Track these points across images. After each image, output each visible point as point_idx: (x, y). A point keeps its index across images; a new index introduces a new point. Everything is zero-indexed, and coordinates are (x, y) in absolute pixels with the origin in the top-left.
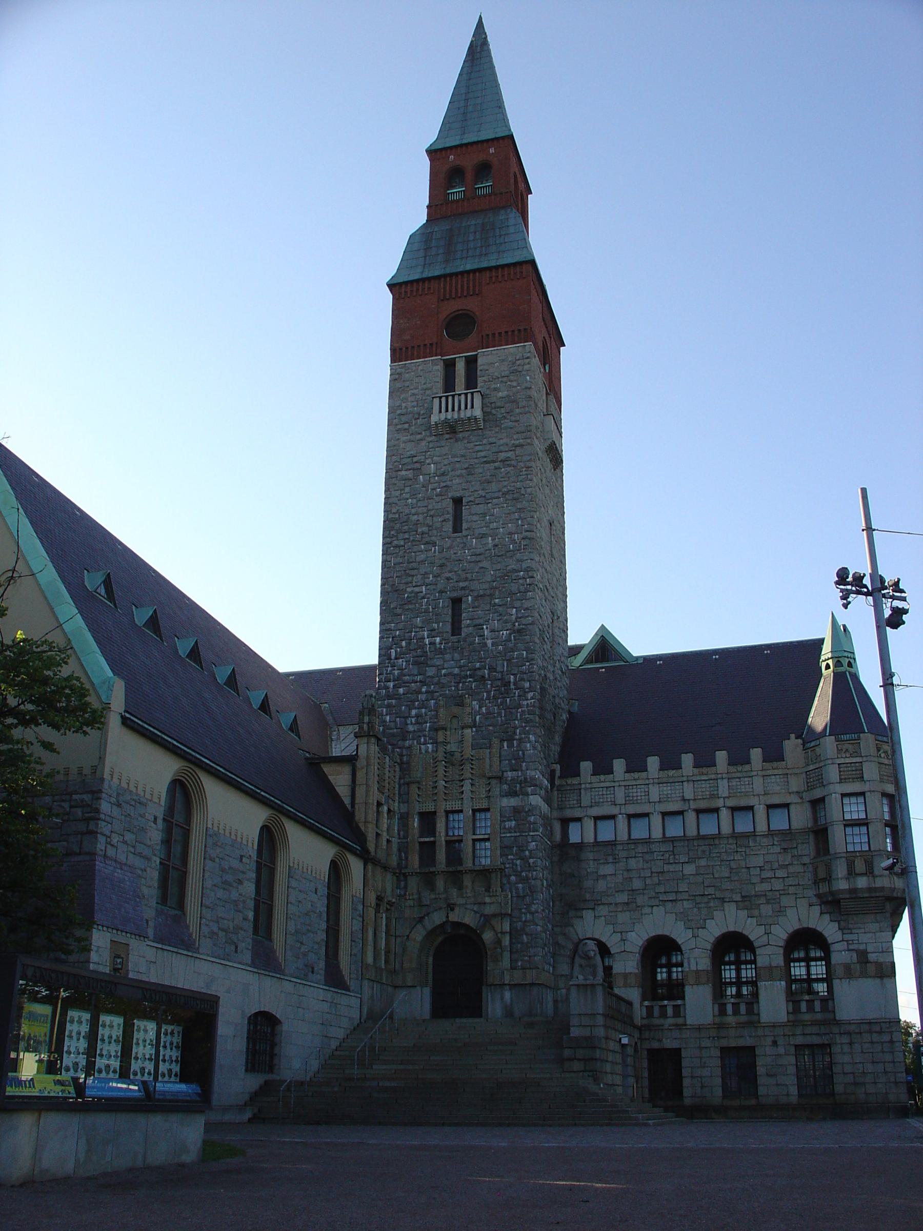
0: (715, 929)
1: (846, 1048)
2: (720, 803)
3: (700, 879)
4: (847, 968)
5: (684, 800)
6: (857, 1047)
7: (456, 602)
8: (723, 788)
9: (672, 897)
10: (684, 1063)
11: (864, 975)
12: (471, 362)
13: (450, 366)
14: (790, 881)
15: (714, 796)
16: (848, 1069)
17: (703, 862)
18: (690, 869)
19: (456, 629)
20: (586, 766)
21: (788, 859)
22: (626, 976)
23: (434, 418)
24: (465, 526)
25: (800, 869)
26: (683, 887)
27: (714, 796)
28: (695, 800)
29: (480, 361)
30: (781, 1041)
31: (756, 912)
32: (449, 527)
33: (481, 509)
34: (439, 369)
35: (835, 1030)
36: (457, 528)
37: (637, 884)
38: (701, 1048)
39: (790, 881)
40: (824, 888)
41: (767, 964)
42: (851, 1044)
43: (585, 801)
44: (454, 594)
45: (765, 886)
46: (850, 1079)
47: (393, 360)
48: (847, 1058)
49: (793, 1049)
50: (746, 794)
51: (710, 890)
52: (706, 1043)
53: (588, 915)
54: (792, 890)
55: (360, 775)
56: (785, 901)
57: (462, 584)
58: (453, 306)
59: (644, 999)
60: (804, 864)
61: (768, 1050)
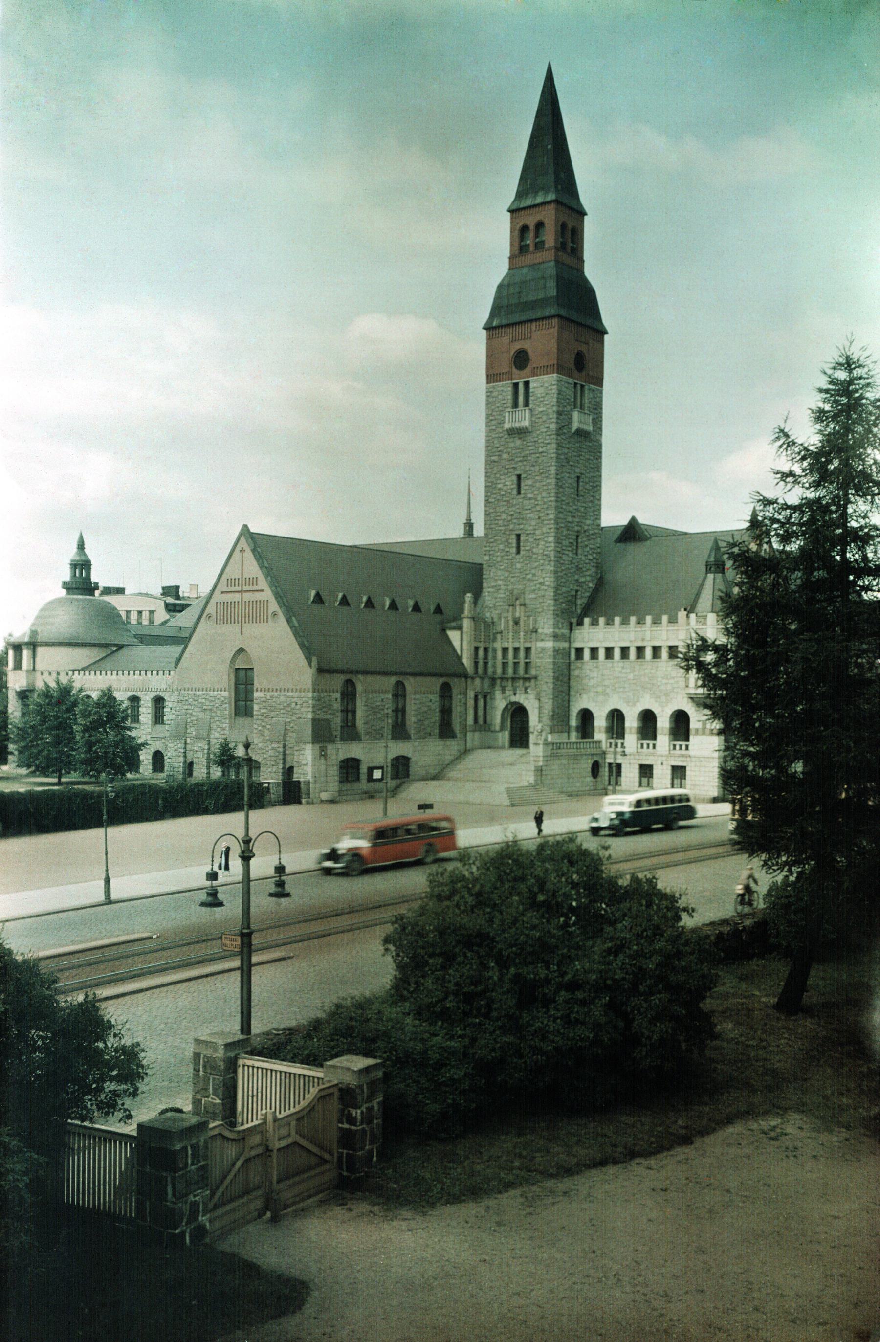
4: (697, 730)
7: (518, 536)
8: (648, 635)
11: (704, 733)
12: (527, 384)
13: (516, 386)
15: (643, 640)
18: (631, 676)
19: (518, 552)
20: (587, 620)
22: (600, 728)
23: (507, 426)
24: (523, 492)
27: (643, 640)
29: (532, 385)
30: (665, 763)
32: (515, 492)
33: (529, 482)
34: (510, 390)
35: (688, 759)
36: (519, 493)
37: (607, 683)
43: (586, 640)
44: (517, 532)
47: (487, 383)
53: (584, 696)
55: (465, 636)
57: (522, 526)
58: (517, 346)
59: (608, 739)
61: (660, 767)
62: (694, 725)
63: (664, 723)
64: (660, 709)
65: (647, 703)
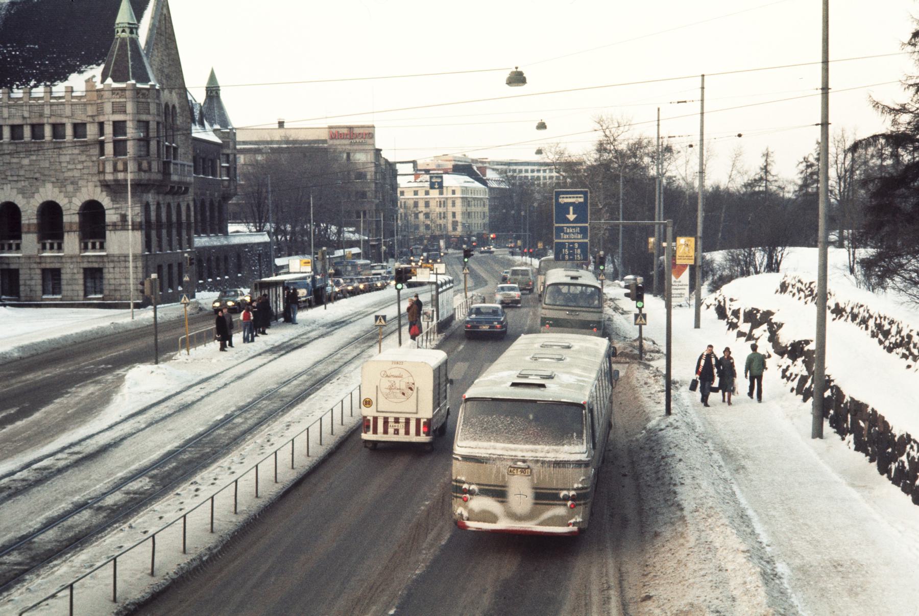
0: (39, 200)
1: (111, 270)
2: (45, 121)
3: (32, 168)
5: (24, 118)
6: (117, 270)
9: (15, 178)
10: (22, 277)
14: (85, 171)
16: (112, 282)
17: (34, 158)
18: (26, 162)
21: (83, 158)
25: (90, 164)
26: (22, 173)
28: (29, 118)
31: (64, 189)
38: (30, 269)
39: (85, 171)
40: (102, 178)
41: (69, 221)
42: (114, 268)
45: (70, 174)
46: (112, 287)
48: (111, 276)
49: (82, 271)
50: (60, 116)
51: (37, 175)
52: (35, 266)
54: (85, 177)
56: (81, 183)
60: (93, 162)
62: (111, 217)
63: (71, 217)
64: (66, 201)
65: (48, 193)
